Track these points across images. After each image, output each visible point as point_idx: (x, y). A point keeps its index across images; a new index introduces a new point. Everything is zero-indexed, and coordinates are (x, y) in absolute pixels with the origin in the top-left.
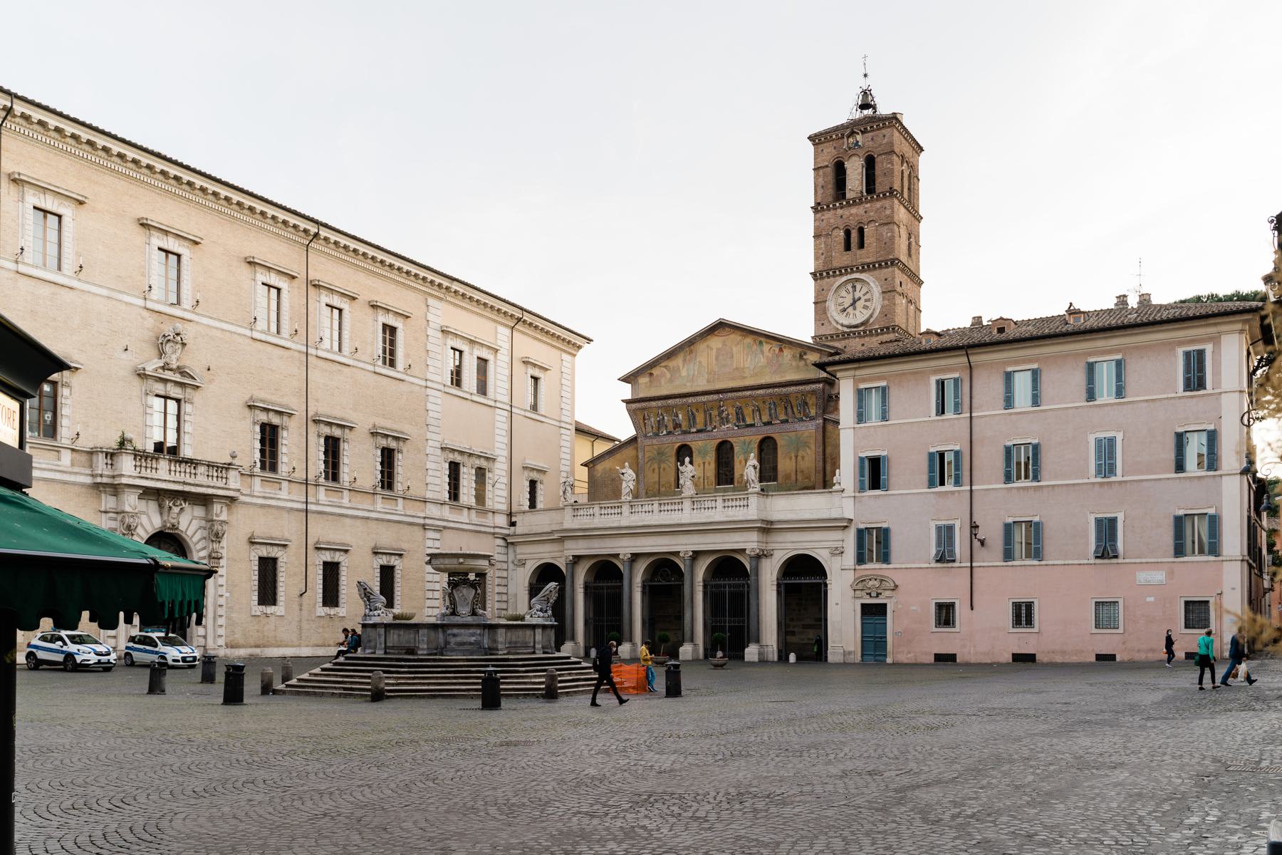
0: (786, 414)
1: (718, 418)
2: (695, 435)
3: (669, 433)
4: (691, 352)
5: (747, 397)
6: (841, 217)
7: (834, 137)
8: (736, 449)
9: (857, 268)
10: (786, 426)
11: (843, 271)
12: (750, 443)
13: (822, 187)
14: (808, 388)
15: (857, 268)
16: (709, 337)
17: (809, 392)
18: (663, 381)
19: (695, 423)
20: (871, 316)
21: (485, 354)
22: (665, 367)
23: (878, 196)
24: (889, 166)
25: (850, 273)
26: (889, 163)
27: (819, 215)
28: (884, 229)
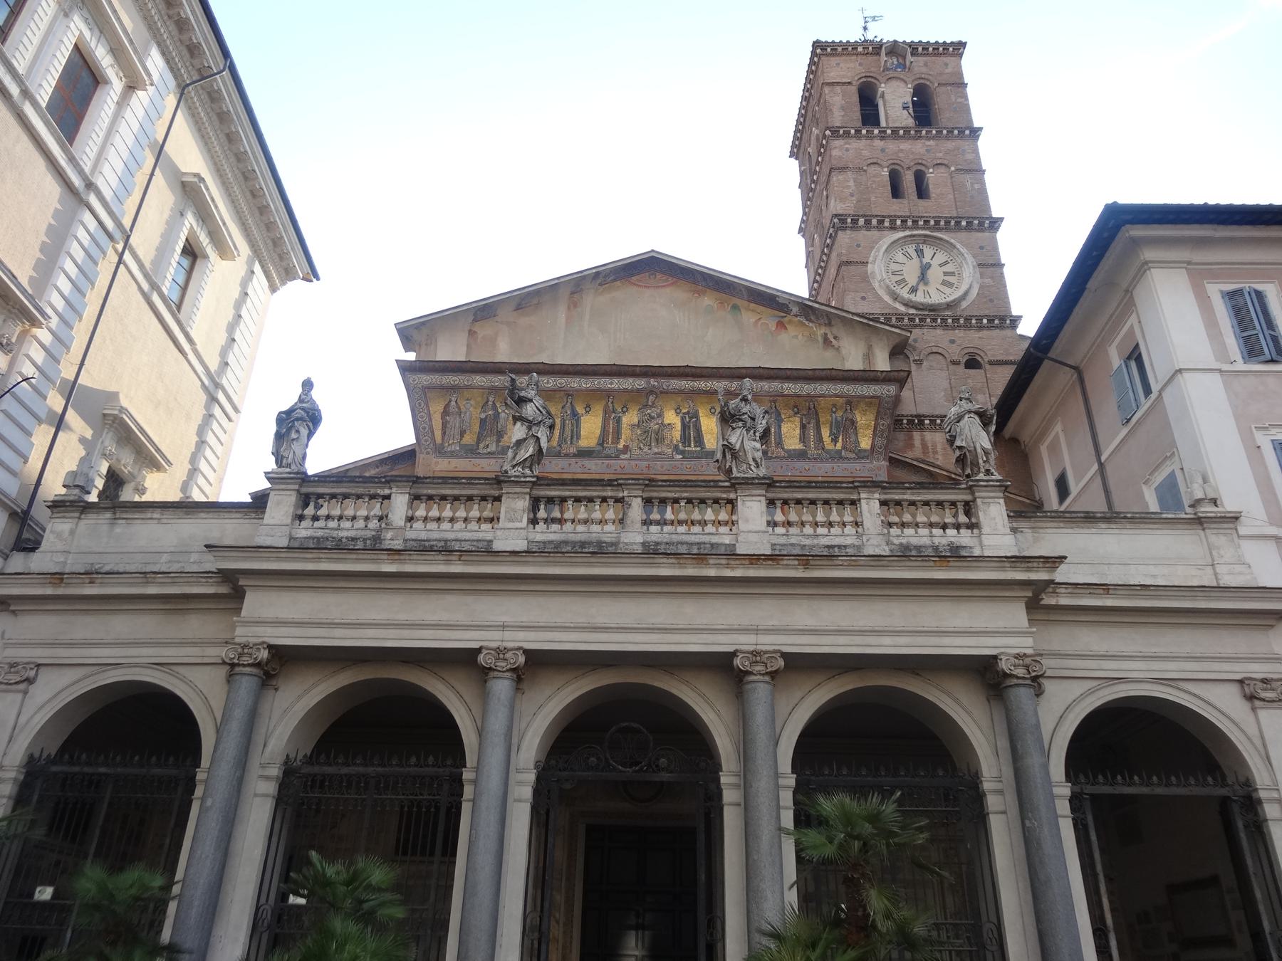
0: (803, 438)
4: (574, 304)
6: (883, 150)
7: (860, 49)
11: (899, 222)
13: (843, 108)
16: (618, 283)
17: (863, 397)
19: (576, 435)
23: (950, 132)
24: (959, 100)
25: (910, 229)
28: (967, 179)
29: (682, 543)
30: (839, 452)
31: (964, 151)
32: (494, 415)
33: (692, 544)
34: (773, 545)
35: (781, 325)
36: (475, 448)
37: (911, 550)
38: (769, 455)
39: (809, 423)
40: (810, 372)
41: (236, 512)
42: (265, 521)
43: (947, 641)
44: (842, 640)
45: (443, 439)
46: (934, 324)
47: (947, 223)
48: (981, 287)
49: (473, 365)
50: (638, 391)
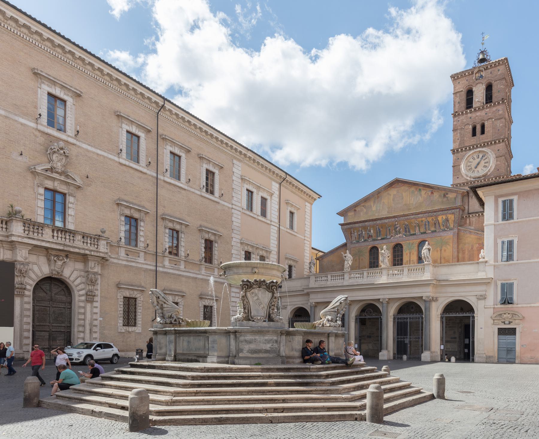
0: (435, 227)
1: (394, 231)
3: (365, 241)
6: (470, 118)
7: (467, 74)
8: (404, 248)
9: (481, 145)
10: (435, 234)
11: (471, 147)
12: (413, 244)
13: (459, 103)
14: (450, 212)
15: (481, 145)
16: (389, 189)
18: (362, 214)
20: (489, 171)
21: (265, 195)
22: (363, 206)
23: (495, 104)
24: (501, 86)
25: (476, 148)
26: (502, 85)
27: (456, 118)
31: (499, 110)
35: (432, 193)
47: (488, 144)
48: (496, 165)
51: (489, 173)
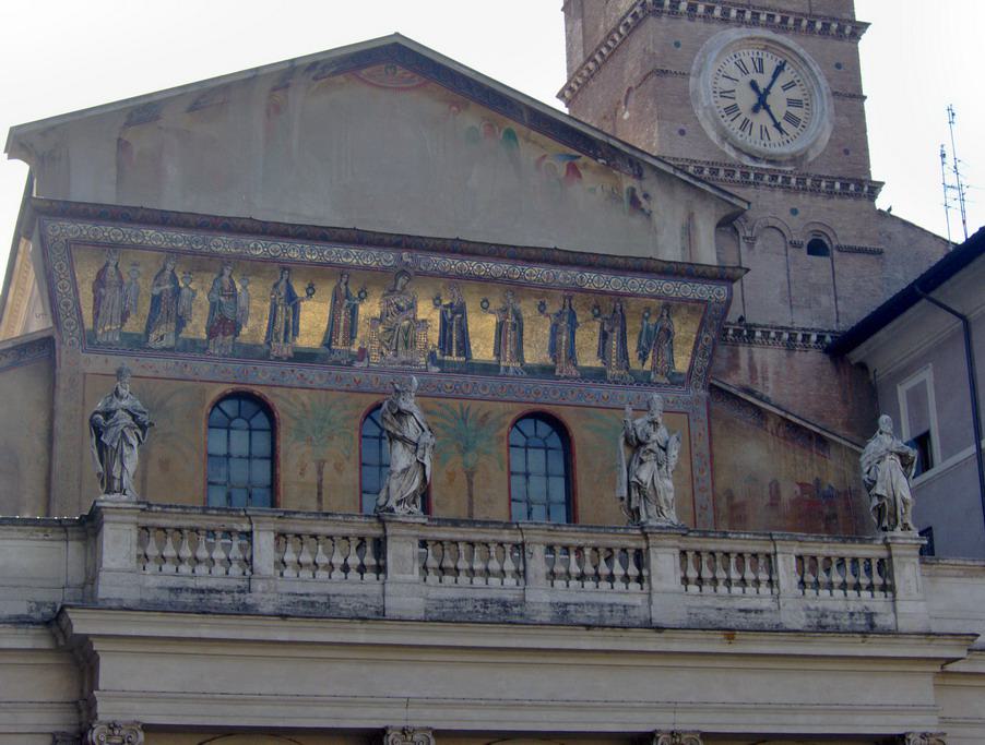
0: (603, 352)
2: (287, 368)
5: (493, 280)
11: (733, 13)
16: (341, 78)
17: (685, 300)
19: (293, 329)
20: (813, 145)
29: (593, 605)
30: (647, 374)
32: (173, 290)
33: (602, 605)
34: (690, 607)
36: (143, 340)
37: (827, 616)
38: (557, 373)
39: (612, 331)
40: (621, 261)
41: (19, 531)
42: (104, 565)
43: (859, 719)
44: (758, 718)
45: (95, 323)
46: (773, 183)
47: (798, 22)
48: (835, 130)
49: (146, 213)
50: (385, 270)
51: (812, 156)
